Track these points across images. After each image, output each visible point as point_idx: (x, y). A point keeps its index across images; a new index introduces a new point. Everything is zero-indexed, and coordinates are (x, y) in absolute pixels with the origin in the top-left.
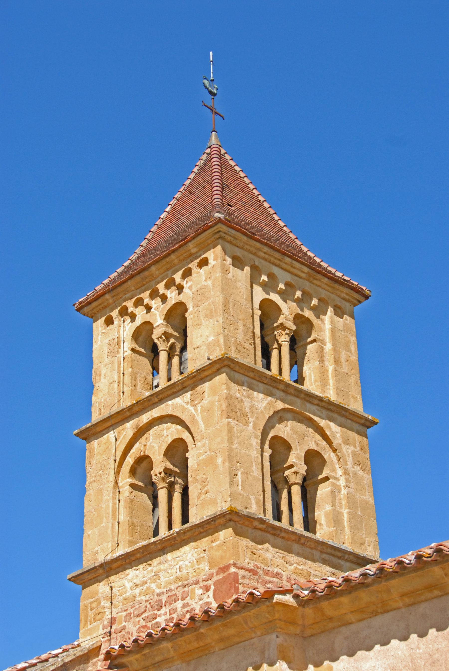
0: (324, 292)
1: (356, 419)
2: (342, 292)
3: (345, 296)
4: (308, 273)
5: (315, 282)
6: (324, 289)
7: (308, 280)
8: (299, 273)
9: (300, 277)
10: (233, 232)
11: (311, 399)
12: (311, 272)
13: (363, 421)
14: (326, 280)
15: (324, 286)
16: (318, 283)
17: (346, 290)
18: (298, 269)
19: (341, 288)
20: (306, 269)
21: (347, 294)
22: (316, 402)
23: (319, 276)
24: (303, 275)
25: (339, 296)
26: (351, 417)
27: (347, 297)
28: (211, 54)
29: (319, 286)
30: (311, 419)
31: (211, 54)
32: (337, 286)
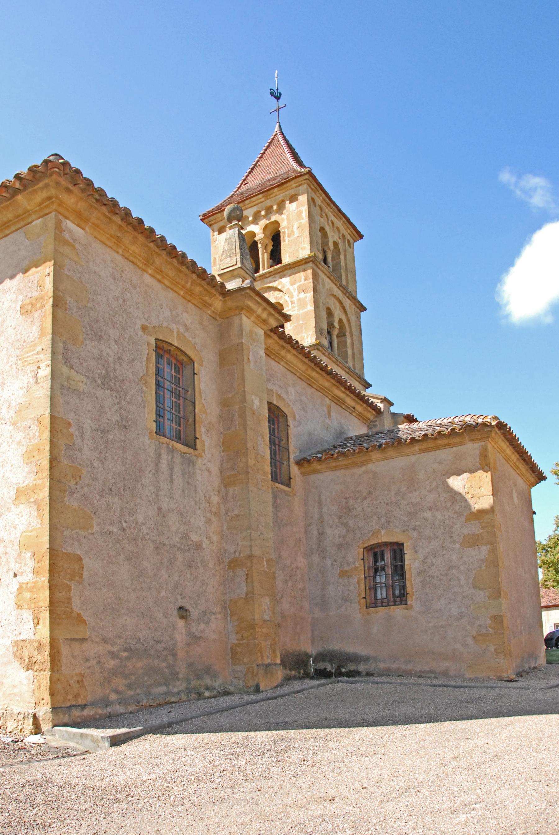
0: (278, 196)
1: (299, 264)
2: (291, 185)
3: (295, 185)
4: (263, 197)
5: (271, 196)
6: (280, 194)
7: (268, 199)
8: (259, 201)
9: (263, 202)
10: (211, 218)
11: (264, 276)
12: (264, 194)
13: (304, 262)
14: (276, 189)
15: (278, 193)
16: (274, 194)
17: (292, 182)
18: (257, 200)
19: (288, 184)
20: (260, 196)
21: (295, 183)
22: (268, 275)
23: (270, 192)
24: (262, 200)
25: (292, 189)
26: (294, 266)
27: (297, 184)
28: (277, 72)
29: (276, 195)
30: (270, 287)
31: (277, 72)
32: (285, 186)
